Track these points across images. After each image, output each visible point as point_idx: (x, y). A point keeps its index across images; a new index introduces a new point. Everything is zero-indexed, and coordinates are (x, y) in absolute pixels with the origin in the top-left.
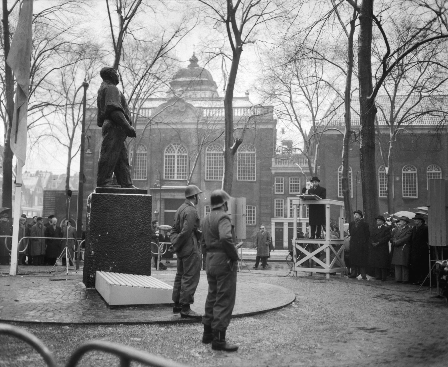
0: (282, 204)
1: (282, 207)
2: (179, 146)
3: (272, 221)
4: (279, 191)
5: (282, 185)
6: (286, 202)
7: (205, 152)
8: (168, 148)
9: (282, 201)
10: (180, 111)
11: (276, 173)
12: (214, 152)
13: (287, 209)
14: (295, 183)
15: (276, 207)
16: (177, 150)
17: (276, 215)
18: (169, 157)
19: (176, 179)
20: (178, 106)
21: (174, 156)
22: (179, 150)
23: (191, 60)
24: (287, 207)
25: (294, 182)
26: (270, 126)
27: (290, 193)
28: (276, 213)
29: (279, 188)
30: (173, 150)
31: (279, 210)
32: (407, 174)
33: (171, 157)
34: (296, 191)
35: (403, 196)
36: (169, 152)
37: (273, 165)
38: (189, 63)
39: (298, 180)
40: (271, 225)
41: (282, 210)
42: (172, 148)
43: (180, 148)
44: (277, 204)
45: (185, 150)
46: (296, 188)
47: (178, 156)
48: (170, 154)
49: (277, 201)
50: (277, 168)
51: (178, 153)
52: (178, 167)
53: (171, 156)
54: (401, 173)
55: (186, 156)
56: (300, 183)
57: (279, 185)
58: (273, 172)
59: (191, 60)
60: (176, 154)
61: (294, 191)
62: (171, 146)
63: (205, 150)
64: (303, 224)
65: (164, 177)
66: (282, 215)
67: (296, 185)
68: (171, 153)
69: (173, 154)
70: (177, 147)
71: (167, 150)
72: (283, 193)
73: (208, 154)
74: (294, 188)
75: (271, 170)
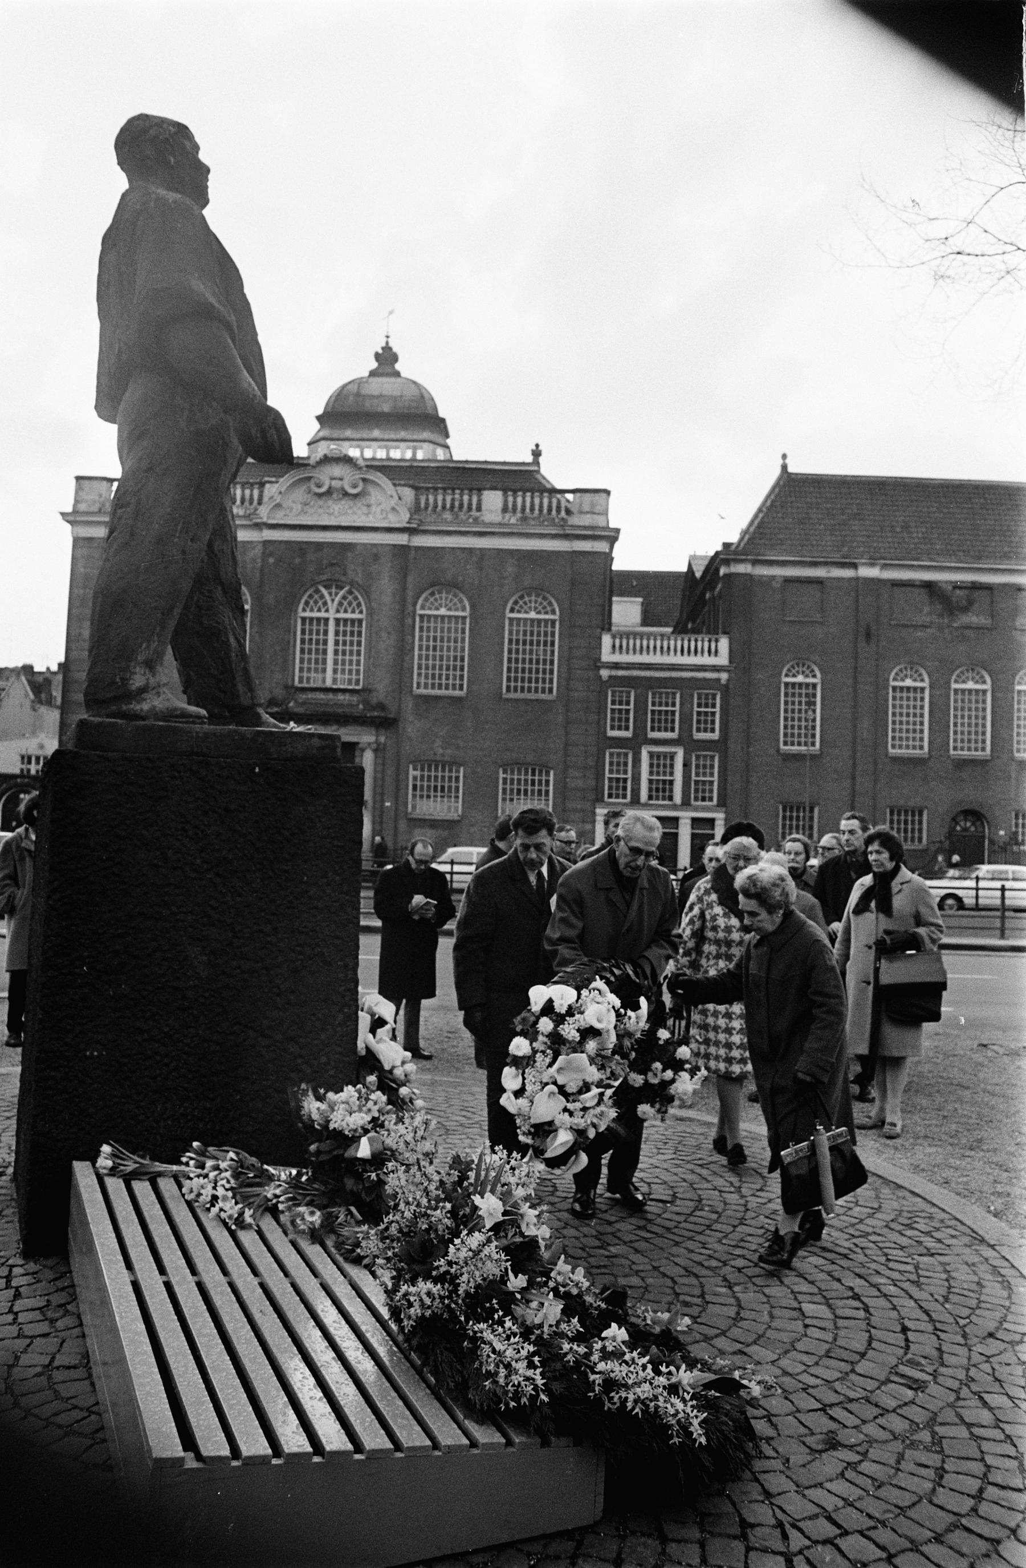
0: (626, 764)
1: (625, 772)
2: (342, 593)
3: (598, 811)
4: (620, 728)
5: (628, 711)
6: (637, 761)
7: (414, 612)
8: (311, 596)
9: (626, 755)
10: (346, 494)
11: (610, 677)
12: (443, 611)
13: (639, 780)
14: (664, 708)
15: (611, 771)
16: (337, 599)
17: (610, 796)
18: (311, 624)
19: (329, 683)
20: (341, 479)
21: (327, 620)
22: (340, 604)
23: (377, 356)
24: (639, 774)
25: (660, 705)
26: (602, 546)
27: (652, 735)
28: (610, 788)
29: (620, 720)
30: (325, 603)
31: (618, 780)
32: (963, 691)
33: (318, 624)
34: (666, 730)
35: (952, 752)
36: (312, 610)
37: (607, 655)
38: (374, 365)
39: (674, 698)
40: (594, 822)
41: (625, 780)
42: (322, 597)
43: (344, 598)
44: (611, 764)
45: (359, 605)
46: (666, 720)
47: (337, 621)
48: (315, 614)
49: (611, 755)
50: (616, 666)
51: (338, 611)
52: (336, 652)
53: (319, 619)
54: (949, 688)
55: (360, 621)
56: (677, 708)
57: (620, 711)
58: (605, 673)
60: (332, 615)
61: (659, 730)
62: (317, 591)
63: (415, 604)
64: (681, 821)
65: (297, 679)
66: (624, 797)
67: (667, 712)
68: (319, 610)
69: (323, 614)
70: (336, 594)
71: (307, 603)
72: (628, 734)
73: (422, 616)
74: (660, 721)
75: (599, 668)
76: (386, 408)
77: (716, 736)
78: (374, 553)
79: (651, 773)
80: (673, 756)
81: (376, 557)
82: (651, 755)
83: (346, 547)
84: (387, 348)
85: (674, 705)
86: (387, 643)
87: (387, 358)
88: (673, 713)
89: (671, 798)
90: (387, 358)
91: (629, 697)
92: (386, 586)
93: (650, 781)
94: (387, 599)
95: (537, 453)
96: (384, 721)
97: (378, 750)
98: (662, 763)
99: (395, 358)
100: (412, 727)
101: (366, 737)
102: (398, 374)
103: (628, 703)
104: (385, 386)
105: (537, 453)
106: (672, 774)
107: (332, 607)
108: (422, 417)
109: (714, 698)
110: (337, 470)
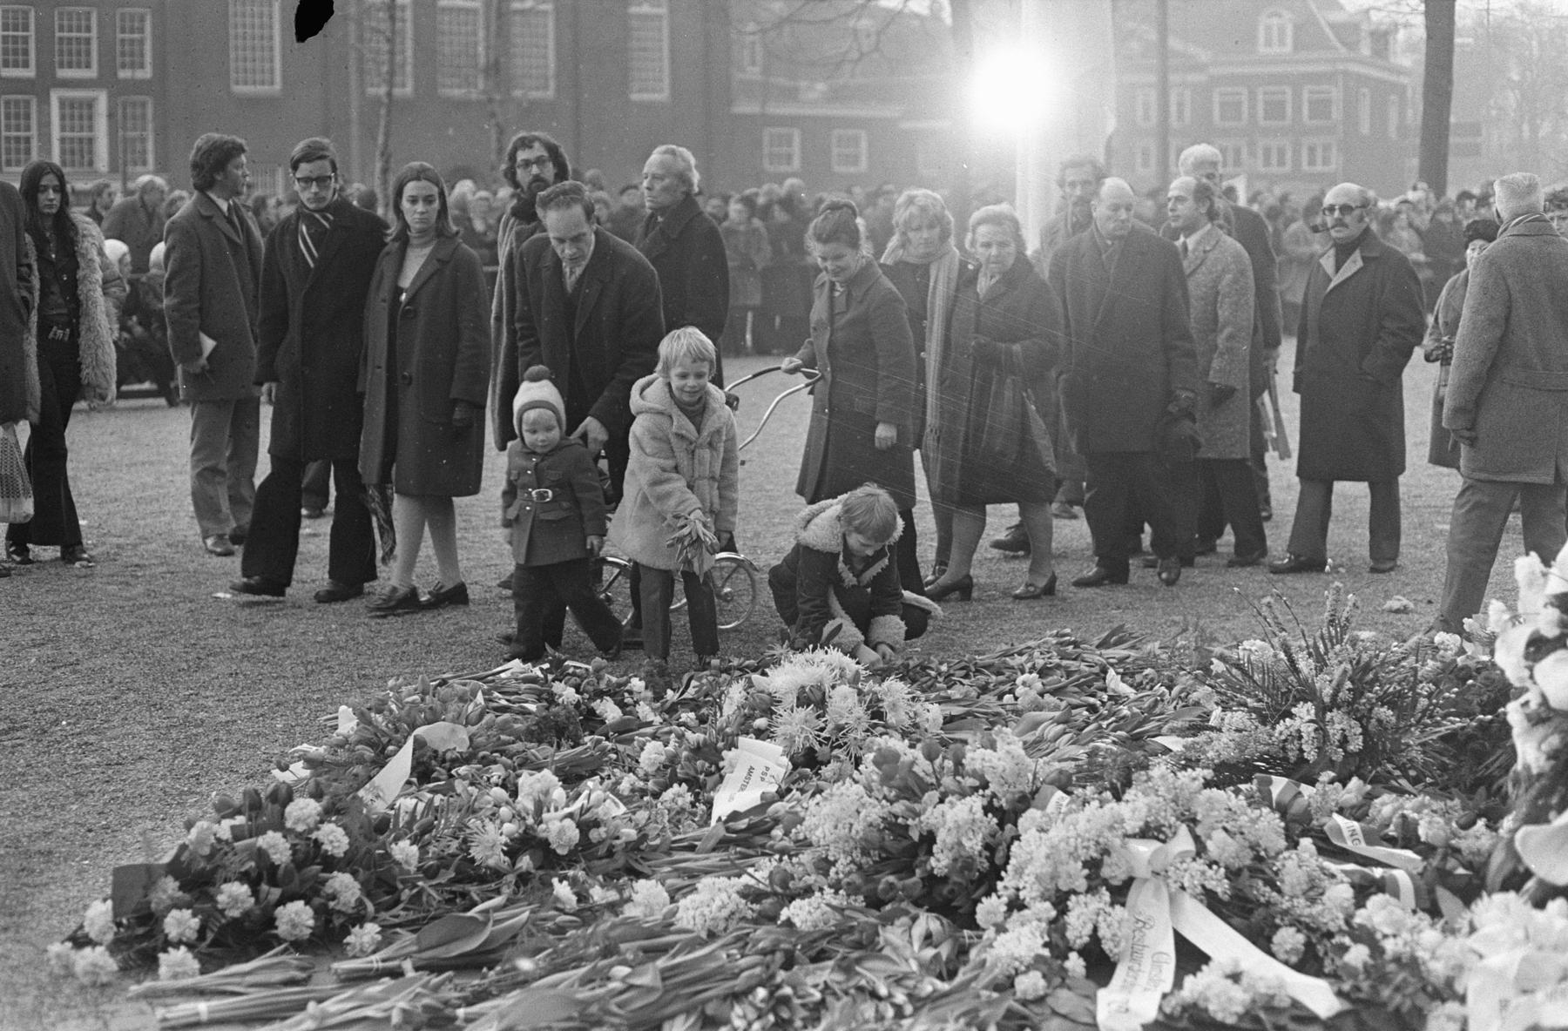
0: (28, 117)
14: (74, 34)
31: (17, 139)
34: (79, 66)
39: (88, 19)
61: (70, 66)
72: (30, 73)
77: (146, 73)
79: (63, 129)
80: (91, 104)
82: (62, 103)
85: (88, 29)
88: (88, 41)
89: (91, 163)
91: (26, 18)
93: (63, 140)
98: (79, 113)
103: (26, 29)
106: (91, 128)
109: (142, 20)
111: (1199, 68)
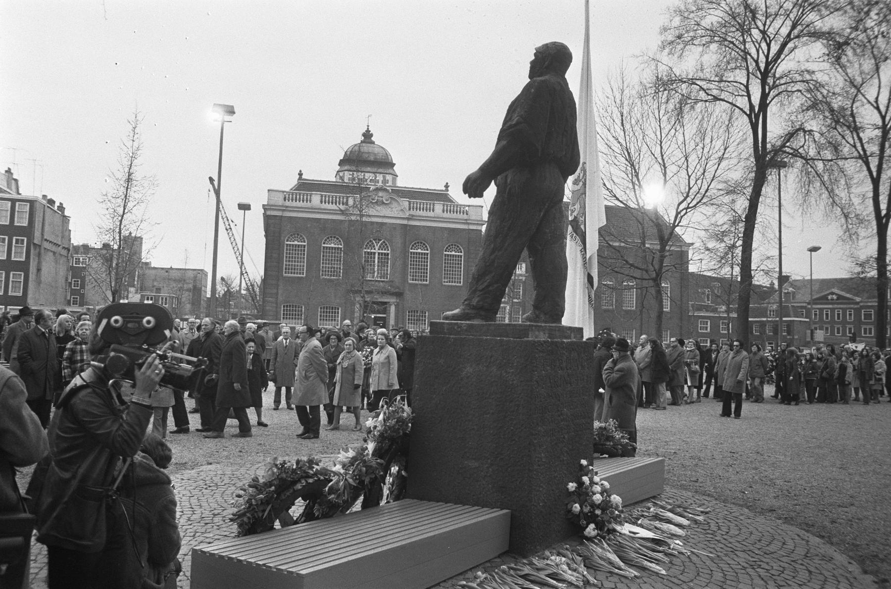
10: (383, 203)
23: (364, 135)
26: (479, 228)
59: (364, 135)
76: (372, 158)
78: (394, 227)
81: (395, 228)
83: (382, 224)
84: (368, 131)
86: (399, 263)
87: (367, 135)
90: (367, 135)
92: (398, 241)
94: (399, 245)
95: (447, 186)
96: (399, 295)
97: (397, 306)
99: (372, 135)
100: (408, 295)
101: (392, 300)
102: (373, 143)
104: (366, 148)
105: (447, 186)
107: (377, 248)
108: (385, 164)
110: (380, 194)
111: (858, 303)
